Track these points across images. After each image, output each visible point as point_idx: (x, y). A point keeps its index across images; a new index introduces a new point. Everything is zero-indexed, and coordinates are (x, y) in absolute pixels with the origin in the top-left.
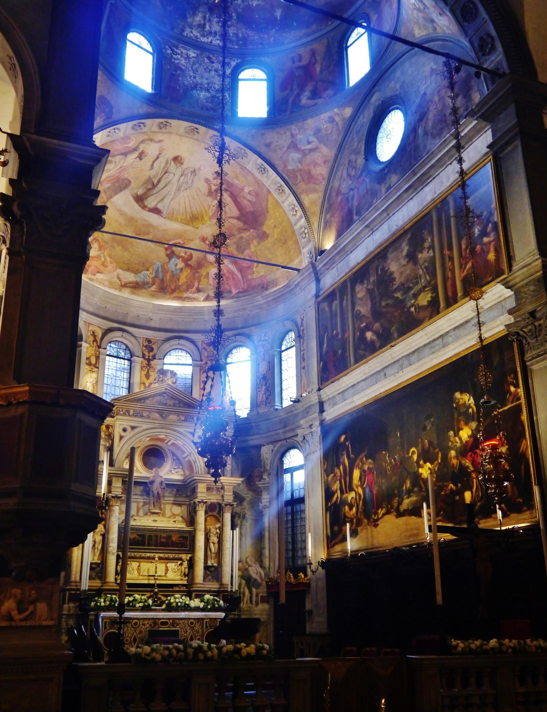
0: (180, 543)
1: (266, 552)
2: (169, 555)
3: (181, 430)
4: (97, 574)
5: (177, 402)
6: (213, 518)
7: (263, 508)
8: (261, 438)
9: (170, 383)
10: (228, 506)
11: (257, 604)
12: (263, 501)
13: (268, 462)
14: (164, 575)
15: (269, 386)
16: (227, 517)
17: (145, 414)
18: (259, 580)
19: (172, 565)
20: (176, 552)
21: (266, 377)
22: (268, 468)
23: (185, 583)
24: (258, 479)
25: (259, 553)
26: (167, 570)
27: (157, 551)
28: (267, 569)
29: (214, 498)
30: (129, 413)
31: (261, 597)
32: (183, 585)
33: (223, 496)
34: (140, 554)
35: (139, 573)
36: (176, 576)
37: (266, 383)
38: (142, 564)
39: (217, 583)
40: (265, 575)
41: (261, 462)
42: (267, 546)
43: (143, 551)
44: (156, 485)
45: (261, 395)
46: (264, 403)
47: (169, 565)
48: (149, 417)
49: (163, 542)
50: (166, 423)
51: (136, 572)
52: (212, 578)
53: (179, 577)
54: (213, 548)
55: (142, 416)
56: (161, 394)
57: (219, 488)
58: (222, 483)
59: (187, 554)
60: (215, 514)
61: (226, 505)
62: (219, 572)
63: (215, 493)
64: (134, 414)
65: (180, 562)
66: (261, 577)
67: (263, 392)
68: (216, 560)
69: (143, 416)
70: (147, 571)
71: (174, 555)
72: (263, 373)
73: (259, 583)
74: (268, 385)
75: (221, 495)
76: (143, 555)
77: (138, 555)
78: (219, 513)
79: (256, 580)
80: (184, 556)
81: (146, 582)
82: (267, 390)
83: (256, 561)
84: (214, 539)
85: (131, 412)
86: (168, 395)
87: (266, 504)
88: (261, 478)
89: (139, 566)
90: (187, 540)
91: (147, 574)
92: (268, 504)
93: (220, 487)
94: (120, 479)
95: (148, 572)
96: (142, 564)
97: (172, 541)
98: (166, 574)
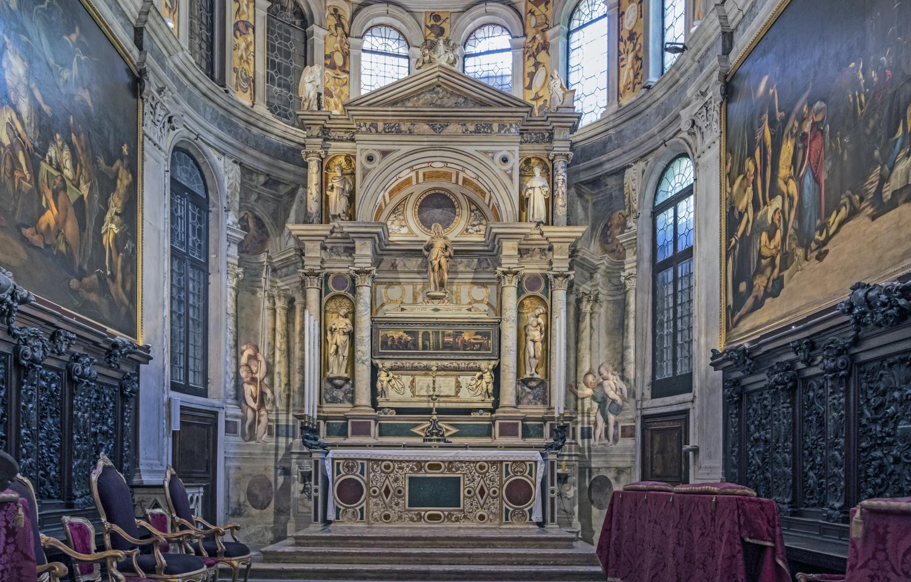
0: (477, 344)
1: (631, 354)
2: (459, 362)
3: (470, 149)
4: (345, 394)
5: (461, 100)
6: (535, 301)
7: (627, 278)
8: (624, 153)
9: (444, 63)
10: (560, 279)
11: (616, 440)
12: (626, 267)
13: (636, 196)
14: (453, 394)
15: (639, 50)
16: (560, 296)
17: (404, 128)
18: (619, 401)
19: (466, 379)
20: (470, 357)
21: (635, 33)
22: (636, 206)
23: (490, 406)
24: (619, 230)
25: (619, 357)
26: (458, 386)
27: (439, 357)
28: (632, 382)
29: (533, 267)
30: (376, 128)
31: (622, 427)
32: (485, 410)
33: (551, 263)
34: (412, 362)
35: (413, 392)
36: (475, 395)
37: (635, 45)
38: (417, 378)
39: (541, 406)
40: (629, 390)
41: (624, 197)
42: (632, 343)
43: (415, 357)
44: (436, 252)
45: (626, 72)
46: (631, 86)
47: (460, 379)
48: (411, 133)
49: (448, 343)
50: (441, 139)
51: (408, 392)
52: (535, 398)
53: (480, 398)
54: (533, 349)
55: (399, 132)
56: (432, 88)
57: (544, 250)
58: (547, 239)
59: (490, 360)
60: (538, 293)
61: (556, 276)
62: (545, 389)
63: (537, 258)
64: (384, 129)
65: (478, 374)
66: (622, 397)
67: (629, 66)
68: (541, 370)
69: (401, 132)
70: (425, 388)
71: (467, 362)
72: (630, 28)
73: (618, 405)
74: (638, 47)
75: (548, 261)
76: (416, 364)
77: (408, 364)
78: (546, 292)
79: (614, 401)
80: (483, 365)
81: (424, 405)
82: (637, 58)
83: (615, 370)
84: (536, 334)
85: (381, 126)
86: (444, 90)
87: (631, 271)
88: (623, 226)
89: (413, 381)
90: (489, 338)
91: (425, 394)
92: (634, 271)
93: (547, 247)
94: (369, 243)
95: (427, 391)
96: (417, 378)
97: (464, 341)
98: (457, 392)
